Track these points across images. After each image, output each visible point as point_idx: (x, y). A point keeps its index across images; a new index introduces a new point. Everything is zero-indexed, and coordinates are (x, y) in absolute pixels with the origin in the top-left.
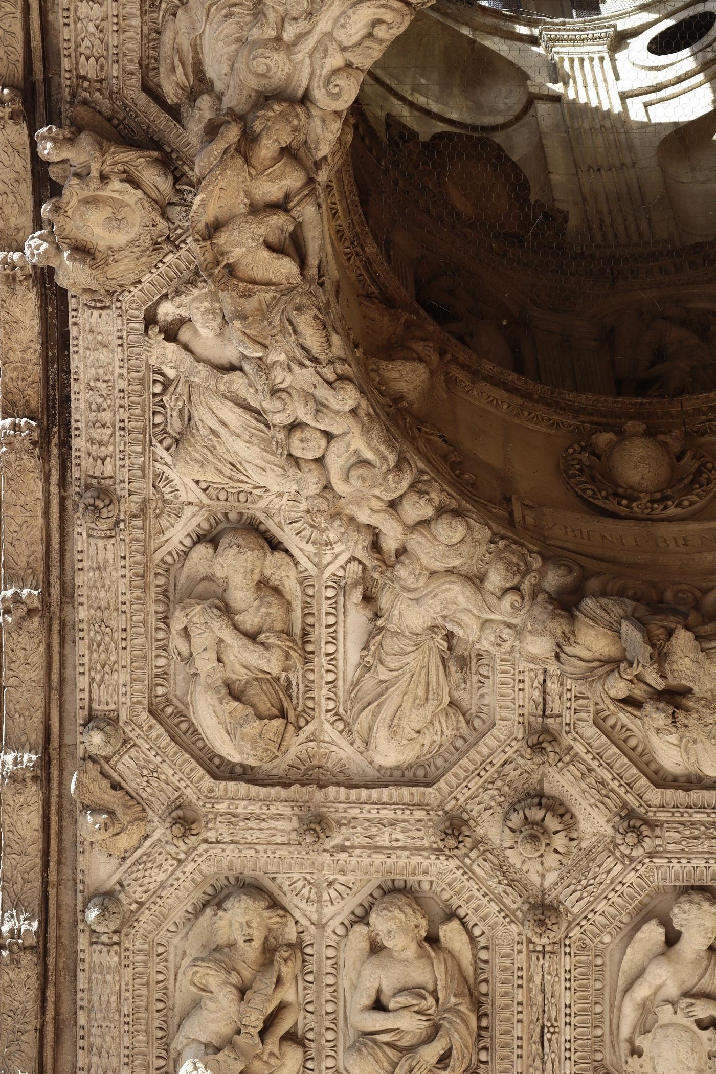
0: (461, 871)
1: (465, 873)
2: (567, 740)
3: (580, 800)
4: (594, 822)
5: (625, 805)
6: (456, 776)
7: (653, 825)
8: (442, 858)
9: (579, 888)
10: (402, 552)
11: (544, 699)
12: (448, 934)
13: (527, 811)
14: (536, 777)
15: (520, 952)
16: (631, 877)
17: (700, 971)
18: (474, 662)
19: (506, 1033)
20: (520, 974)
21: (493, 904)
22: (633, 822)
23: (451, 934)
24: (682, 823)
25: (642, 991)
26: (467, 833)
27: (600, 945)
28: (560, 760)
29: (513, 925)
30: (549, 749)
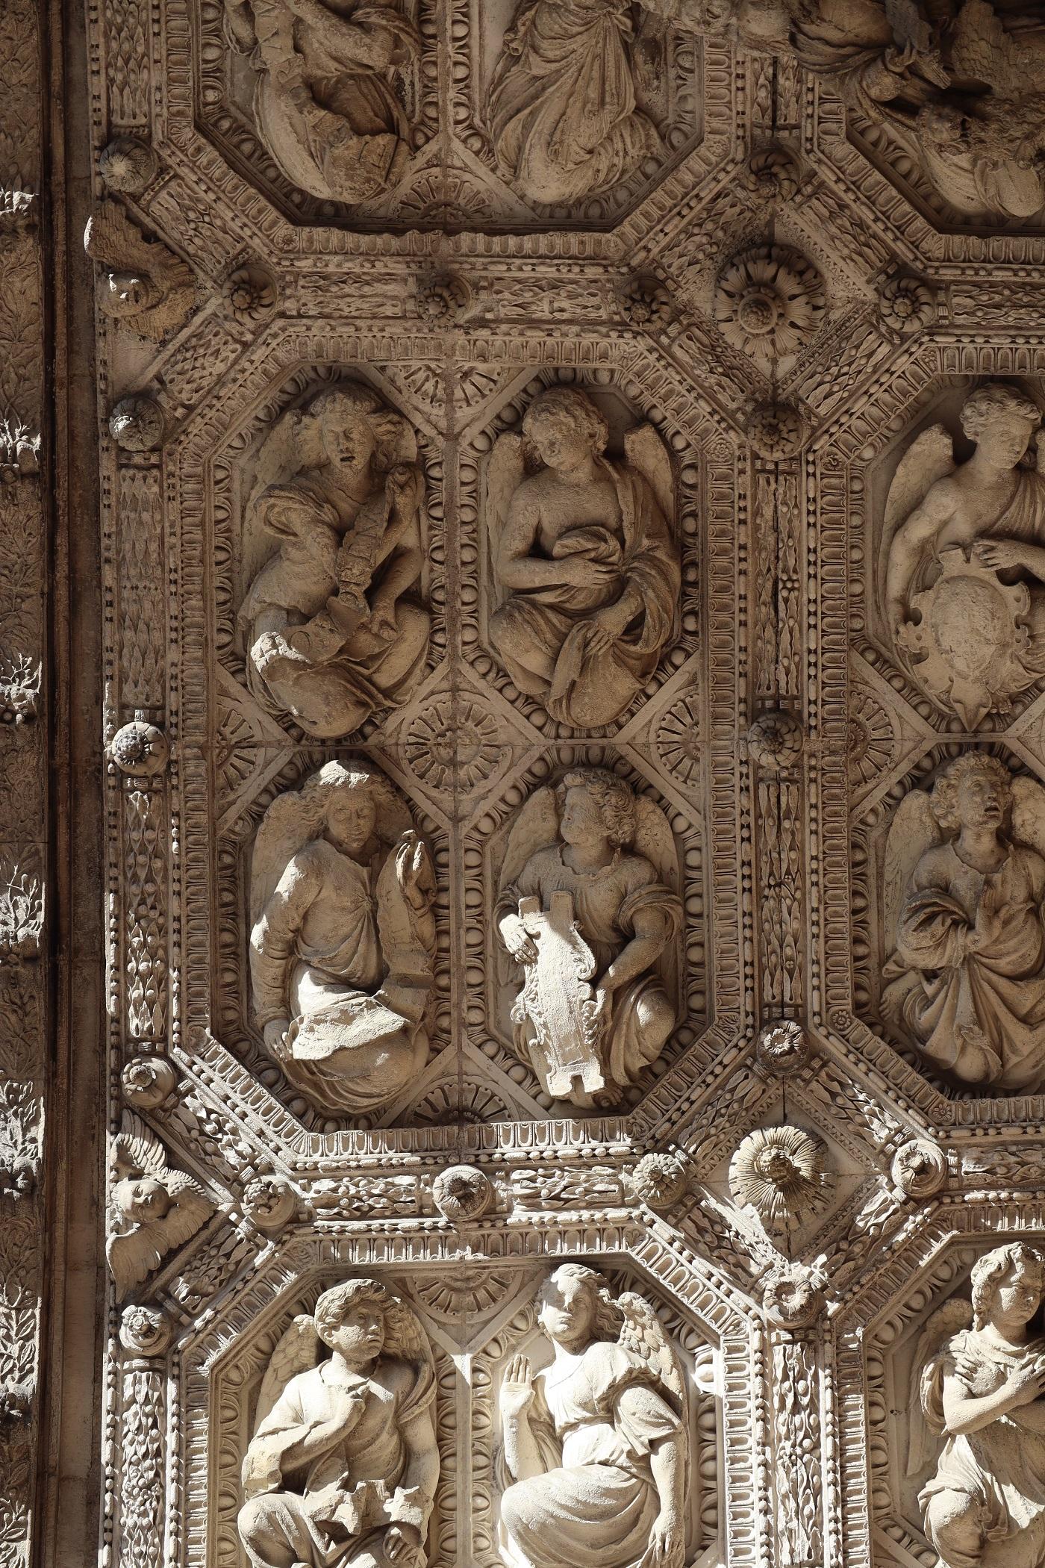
0: (656, 355)
1: (660, 358)
2: (809, 162)
3: (828, 251)
4: (849, 283)
5: (893, 257)
6: (646, 215)
7: (935, 287)
8: (628, 335)
9: (828, 378)
11: (774, 102)
12: (638, 447)
13: (751, 267)
14: (763, 217)
15: (742, 472)
16: (903, 363)
17: (1004, 500)
18: (670, 48)
19: (724, 589)
20: (742, 504)
21: (702, 403)
22: (906, 283)
23: (642, 447)
24: (975, 284)
25: (919, 529)
26: (664, 299)
27: (858, 463)
28: (799, 192)
29: (732, 433)
30: (783, 175)
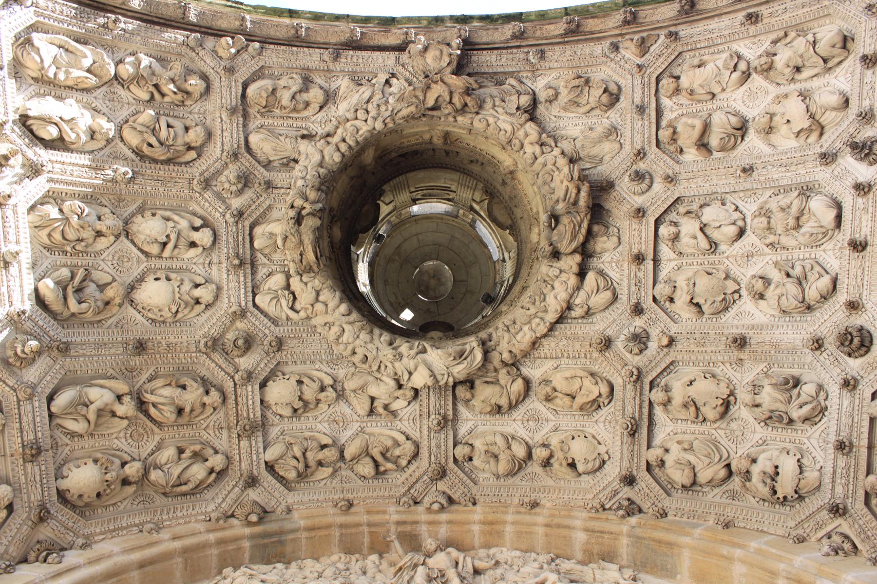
10: (328, 143)
23: (193, 154)
